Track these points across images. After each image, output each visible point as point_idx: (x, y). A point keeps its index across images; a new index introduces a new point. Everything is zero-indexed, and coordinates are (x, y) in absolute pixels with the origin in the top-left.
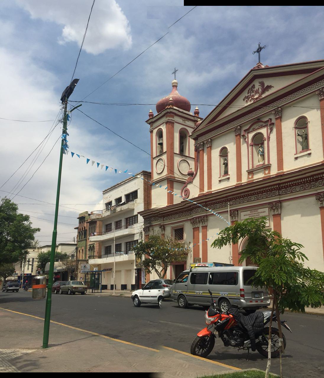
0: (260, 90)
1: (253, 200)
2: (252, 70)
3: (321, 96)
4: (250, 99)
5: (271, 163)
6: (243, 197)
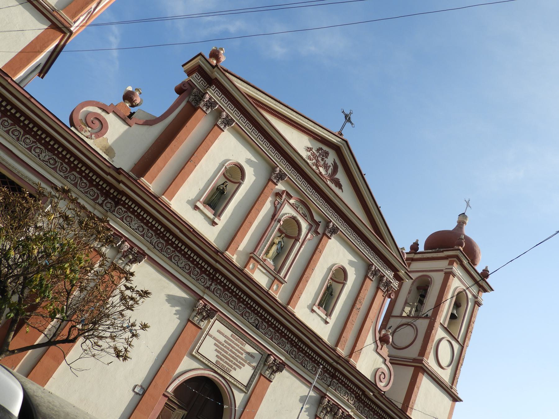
0: (330, 171)
1: (250, 321)
2: (346, 142)
5: (286, 279)
6: (239, 299)
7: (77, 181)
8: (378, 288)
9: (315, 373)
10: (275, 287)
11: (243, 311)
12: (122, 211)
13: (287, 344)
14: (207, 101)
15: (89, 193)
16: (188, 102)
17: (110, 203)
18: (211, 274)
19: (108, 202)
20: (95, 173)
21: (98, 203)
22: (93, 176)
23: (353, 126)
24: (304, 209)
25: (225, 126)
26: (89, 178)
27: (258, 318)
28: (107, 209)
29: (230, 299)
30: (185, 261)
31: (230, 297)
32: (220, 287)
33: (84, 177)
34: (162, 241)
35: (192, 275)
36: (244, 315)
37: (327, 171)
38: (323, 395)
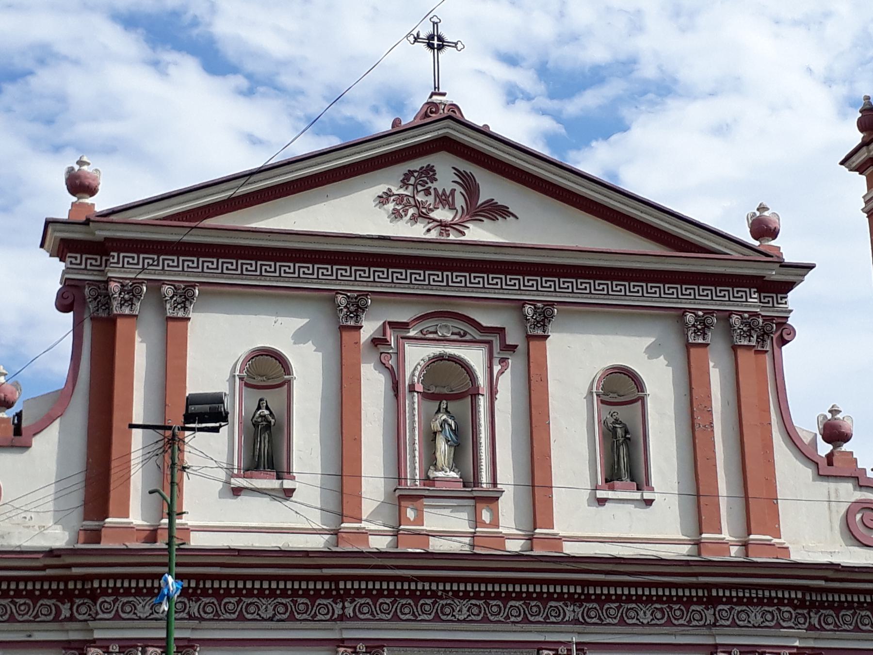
0: (460, 202)
1: (462, 617)
3: (695, 333)
4: (411, 211)
6: (412, 594)
7: (11, 608)
8: (735, 348)
9: (665, 619)
10: (486, 516)
11: (435, 611)
12: (110, 604)
13: (565, 608)
14: (120, 294)
15: (42, 614)
16: (92, 319)
17: (84, 604)
18: (330, 590)
19: (78, 606)
20: (26, 579)
21: (67, 620)
22: (26, 586)
23: (459, 46)
24: (450, 324)
25: (185, 308)
26: (24, 593)
27: (473, 602)
28: (85, 617)
29: (395, 607)
30: (269, 602)
31: (393, 603)
32: (363, 601)
33: (15, 596)
34: (206, 600)
35: (298, 616)
36: (440, 615)
37: (452, 208)
38: (713, 650)
